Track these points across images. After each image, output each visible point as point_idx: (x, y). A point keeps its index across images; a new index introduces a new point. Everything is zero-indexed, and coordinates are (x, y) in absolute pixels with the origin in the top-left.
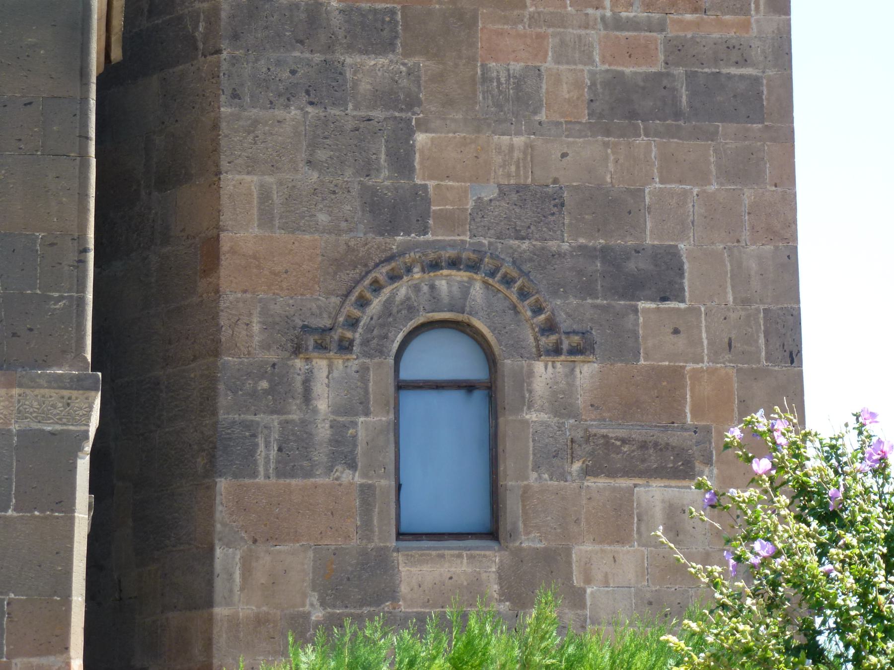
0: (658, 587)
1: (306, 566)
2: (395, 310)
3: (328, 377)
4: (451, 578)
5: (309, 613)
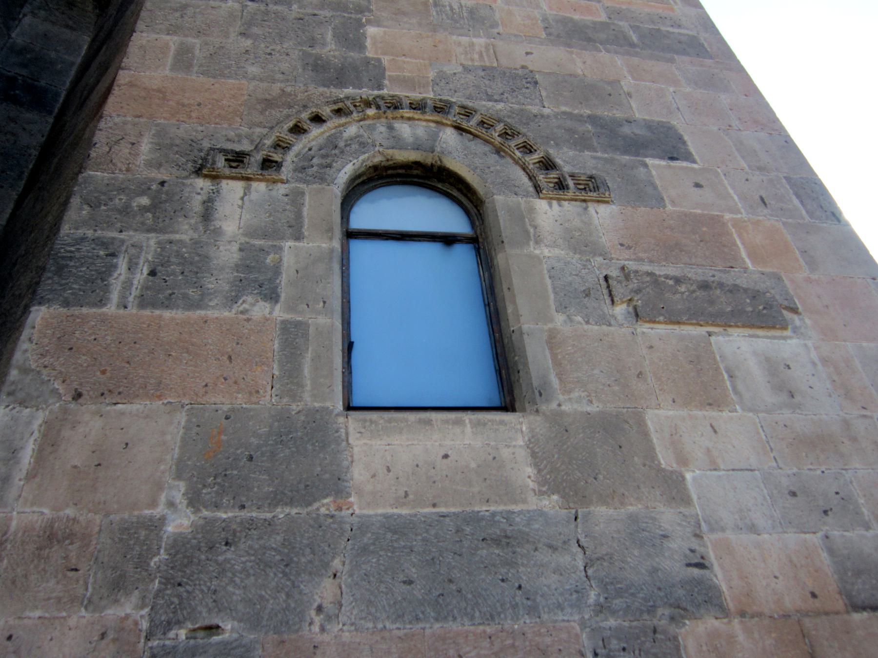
0: (795, 470)
1: (169, 437)
2: (341, 144)
3: (242, 199)
4: (446, 456)
5: (163, 519)
